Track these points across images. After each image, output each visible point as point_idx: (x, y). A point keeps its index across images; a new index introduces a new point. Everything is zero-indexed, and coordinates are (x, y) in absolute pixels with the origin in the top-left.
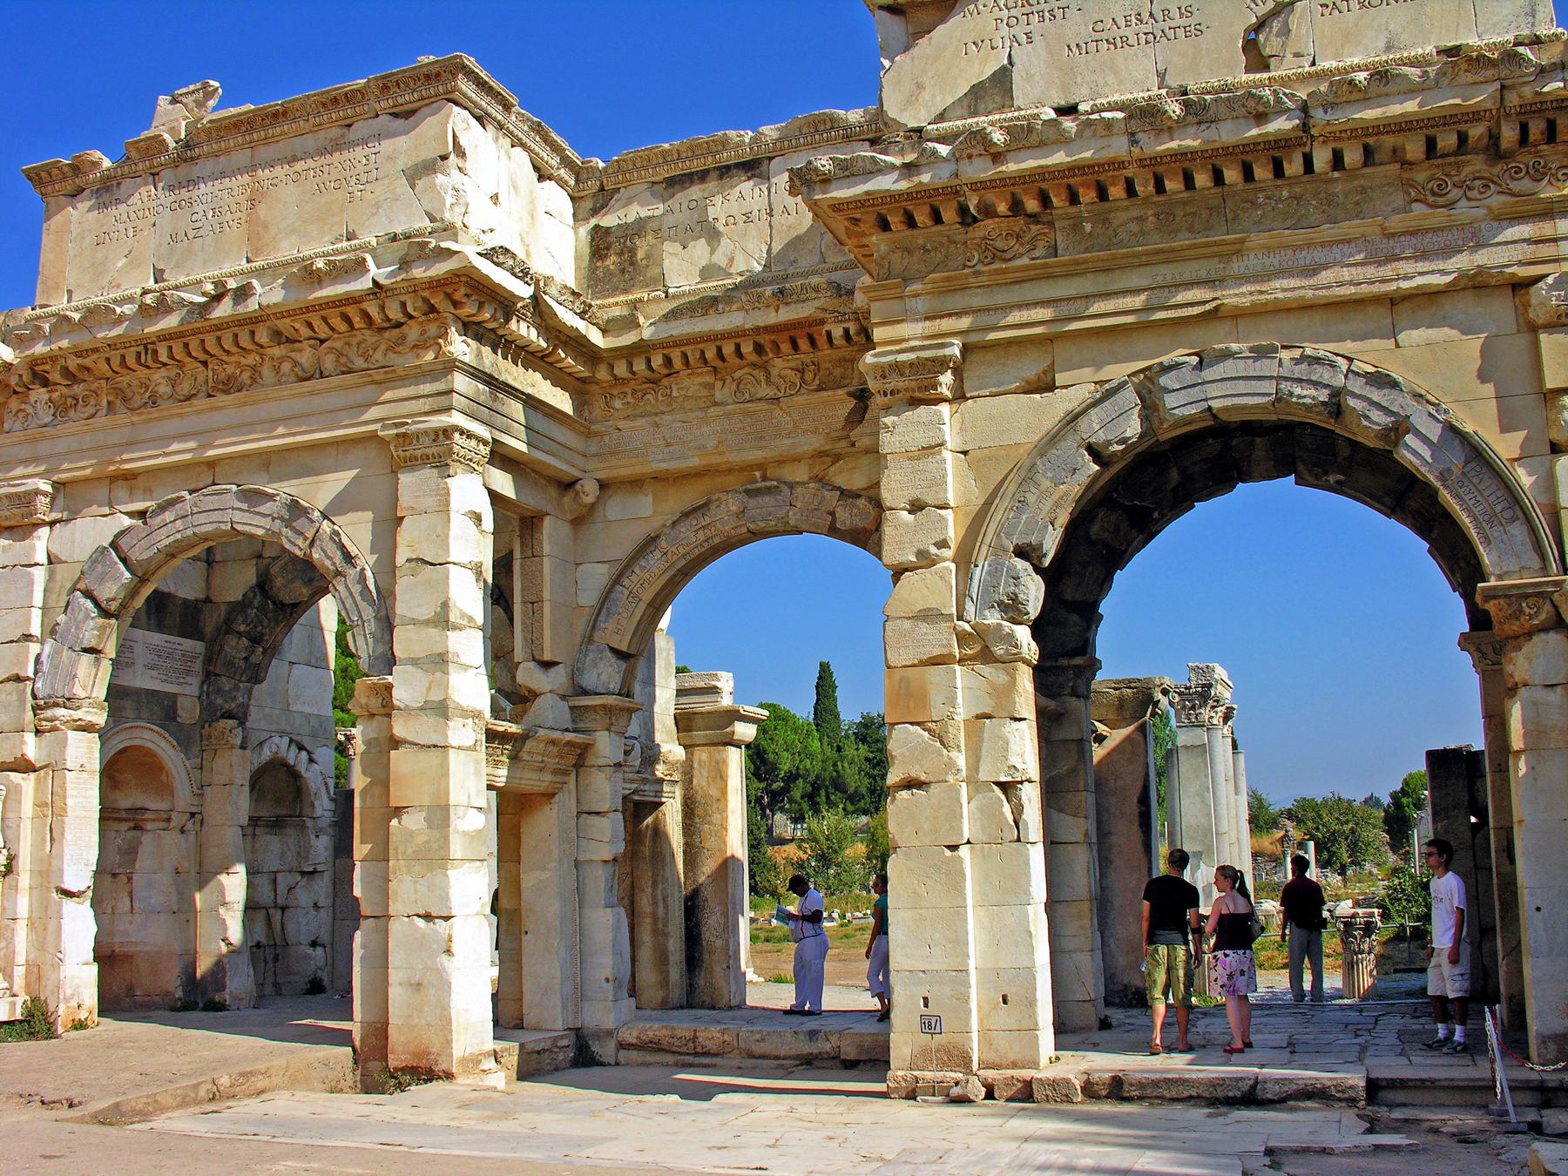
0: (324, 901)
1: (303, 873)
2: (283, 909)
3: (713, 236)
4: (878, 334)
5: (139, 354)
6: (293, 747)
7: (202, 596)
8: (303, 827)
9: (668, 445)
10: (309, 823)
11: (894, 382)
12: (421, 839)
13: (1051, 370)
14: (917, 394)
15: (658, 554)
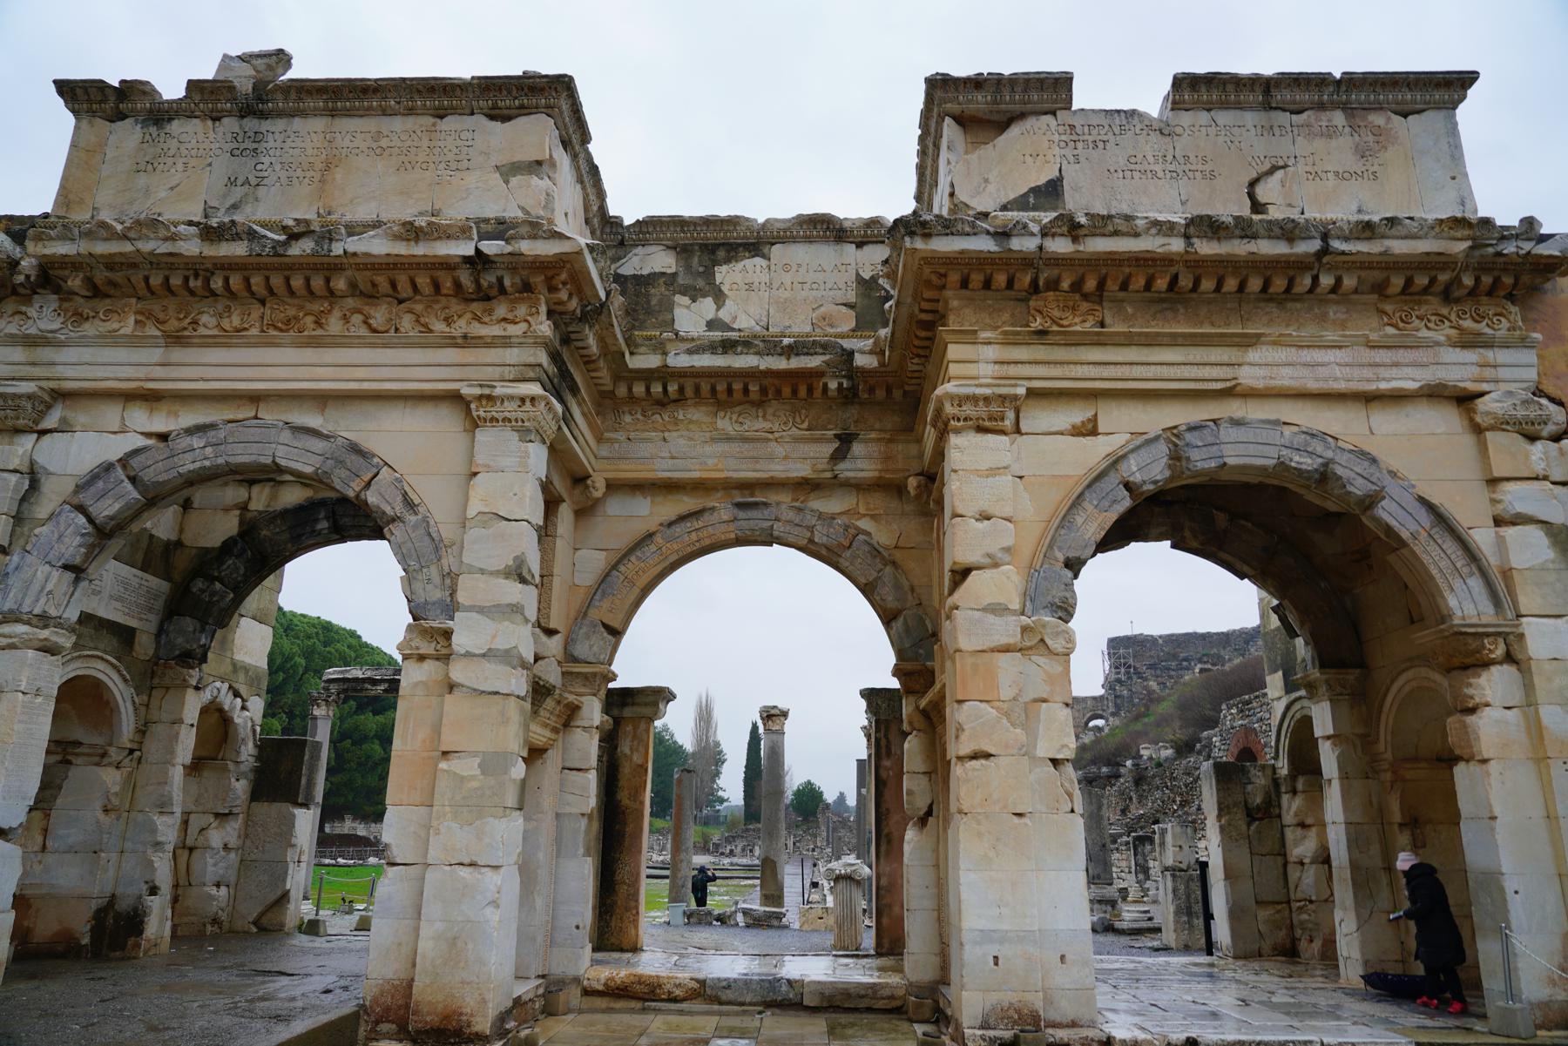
0: (233, 841)
1: (217, 815)
2: (191, 850)
3: (719, 297)
4: (953, 369)
5: (186, 279)
6: (230, 694)
7: (174, 537)
8: (225, 769)
9: (673, 458)
10: (231, 766)
11: (968, 409)
12: (475, 784)
13: (1094, 419)
14: (987, 424)
15: (653, 548)
